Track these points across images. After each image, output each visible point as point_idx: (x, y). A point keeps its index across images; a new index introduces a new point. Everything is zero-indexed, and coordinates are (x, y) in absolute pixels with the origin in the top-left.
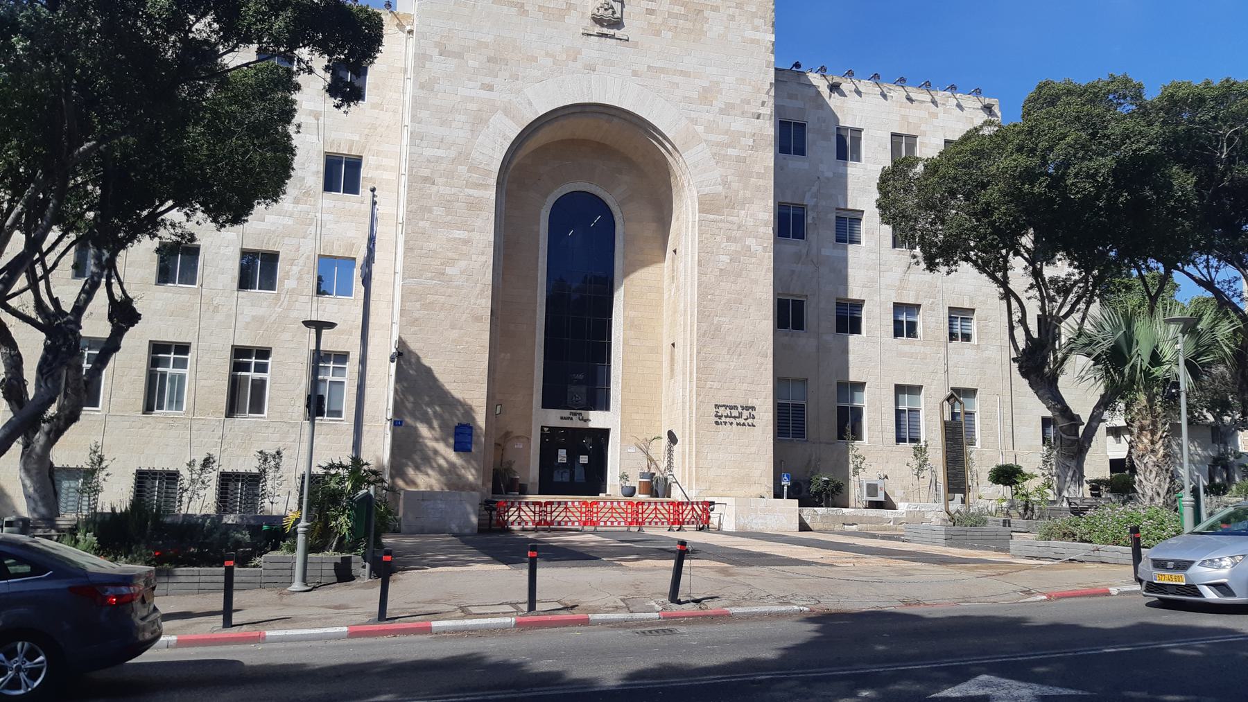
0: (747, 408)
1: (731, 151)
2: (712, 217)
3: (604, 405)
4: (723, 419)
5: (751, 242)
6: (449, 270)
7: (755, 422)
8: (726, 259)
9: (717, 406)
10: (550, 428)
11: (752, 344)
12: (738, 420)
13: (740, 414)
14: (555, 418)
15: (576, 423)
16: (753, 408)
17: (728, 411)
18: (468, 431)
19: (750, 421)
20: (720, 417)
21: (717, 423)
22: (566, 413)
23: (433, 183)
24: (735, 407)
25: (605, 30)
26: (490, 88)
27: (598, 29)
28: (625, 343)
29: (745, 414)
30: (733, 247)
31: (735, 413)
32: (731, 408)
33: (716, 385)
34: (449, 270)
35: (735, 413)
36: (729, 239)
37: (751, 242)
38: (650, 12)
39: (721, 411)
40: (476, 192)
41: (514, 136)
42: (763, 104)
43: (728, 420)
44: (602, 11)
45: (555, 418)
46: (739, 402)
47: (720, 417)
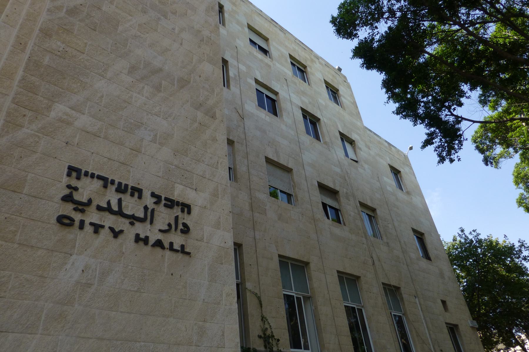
0: (171, 204)
4: (93, 216)
11: (183, 83)
12: (142, 229)
16: (186, 208)
17: (113, 197)
19: (177, 240)
21: (64, 221)
24: (137, 192)
29: (164, 216)
31: (132, 206)
32: (121, 189)
33: (83, 121)
35: (132, 206)
43: (109, 220)
47: (81, 207)
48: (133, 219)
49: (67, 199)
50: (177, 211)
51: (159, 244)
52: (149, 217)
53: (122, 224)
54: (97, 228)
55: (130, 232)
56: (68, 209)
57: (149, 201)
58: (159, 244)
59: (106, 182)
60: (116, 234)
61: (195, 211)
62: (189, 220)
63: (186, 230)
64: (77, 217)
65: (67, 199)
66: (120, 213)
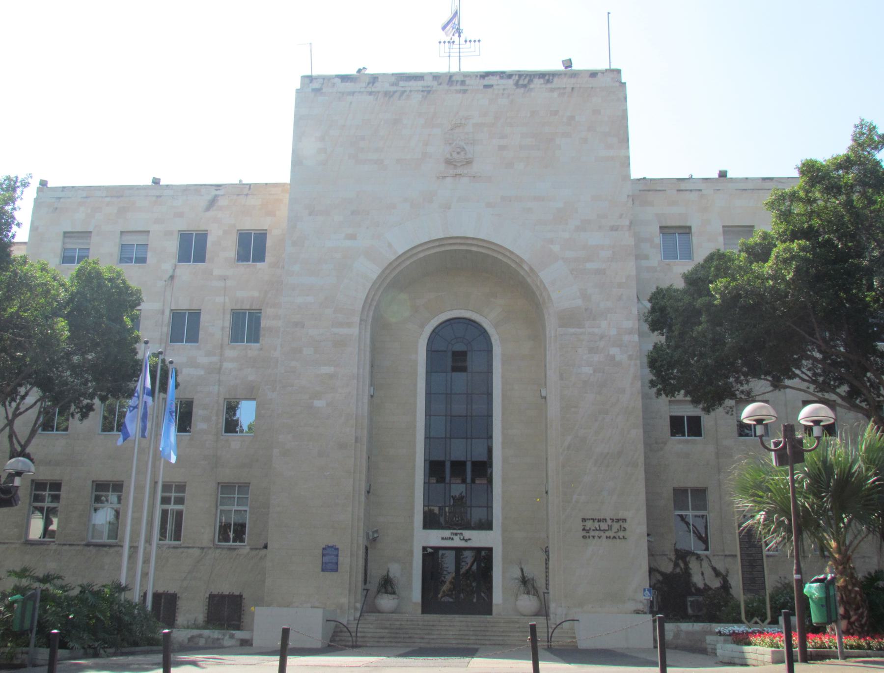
0: (618, 520)
1: (589, 266)
2: (572, 330)
3: (487, 525)
4: (592, 533)
5: (614, 351)
6: (318, 403)
7: (627, 534)
8: (588, 370)
9: (584, 520)
10: (431, 548)
12: (608, 534)
13: (610, 528)
14: (436, 538)
15: (457, 543)
16: (624, 520)
17: (597, 525)
18: (335, 553)
19: (621, 534)
20: (588, 531)
22: (447, 533)
23: (303, 327)
25: (459, 171)
26: (352, 237)
27: (451, 172)
28: (505, 460)
29: (616, 526)
30: (596, 358)
32: (599, 521)
34: (318, 403)
35: (604, 526)
36: (592, 350)
37: (614, 351)
38: (502, 148)
39: (589, 524)
40: (343, 331)
41: (375, 276)
42: (621, 216)
43: (597, 533)
44: (455, 155)
45: (436, 538)
46: (608, 512)
48: (604, 530)
49: (584, 530)
50: (621, 523)
51: (614, 537)
52: (610, 528)
53: (602, 533)
54: (594, 537)
55: (604, 535)
56: (584, 533)
57: (609, 522)
58: (614, 537)
59: (593, 520)
60: (600, 537)
61: (628, 521)
62: (625, 525)
63: (625, 529)
64: (587, 535)
65: (584, 530)
66: (600, 530)
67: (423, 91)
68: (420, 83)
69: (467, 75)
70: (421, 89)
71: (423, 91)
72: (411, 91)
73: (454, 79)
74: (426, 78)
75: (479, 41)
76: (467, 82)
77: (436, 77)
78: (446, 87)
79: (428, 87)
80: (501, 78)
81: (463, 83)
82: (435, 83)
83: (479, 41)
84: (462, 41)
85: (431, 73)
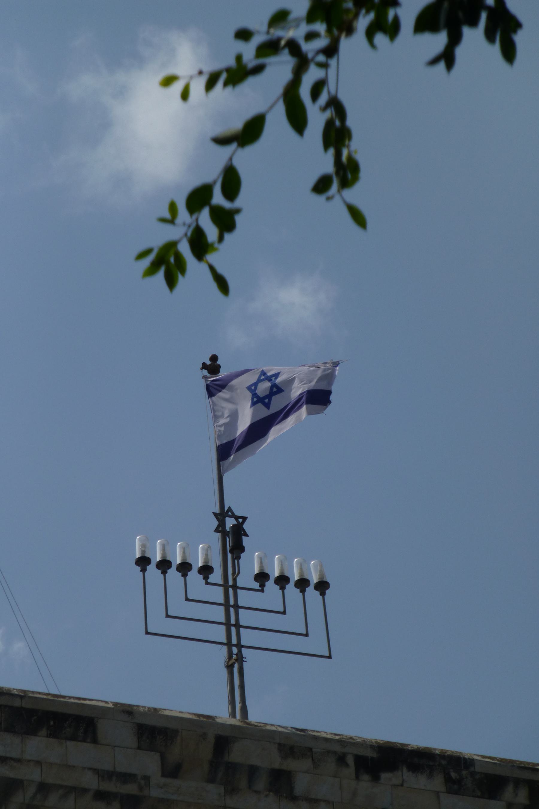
67: (101, 796)
68: (79, 753)
69: (297, 746)
70: (90, 781)
71: (101, 796)
72: (44, 788)
73: (237, 754)
74: (104, 727)
75: (322, 586)
76: (301, 783)
77: (153, 731)
78: (213, 792)
79: (126, 778)
80: (454, 786)
81: (280, 782)
82: (149, 764)
83: (322, 586)
84: (245, 579)
85: (128, 711)
